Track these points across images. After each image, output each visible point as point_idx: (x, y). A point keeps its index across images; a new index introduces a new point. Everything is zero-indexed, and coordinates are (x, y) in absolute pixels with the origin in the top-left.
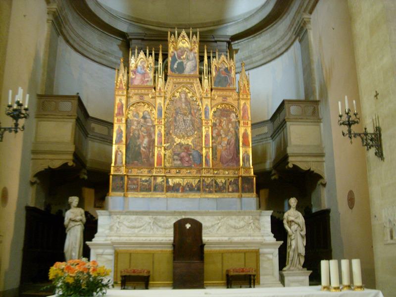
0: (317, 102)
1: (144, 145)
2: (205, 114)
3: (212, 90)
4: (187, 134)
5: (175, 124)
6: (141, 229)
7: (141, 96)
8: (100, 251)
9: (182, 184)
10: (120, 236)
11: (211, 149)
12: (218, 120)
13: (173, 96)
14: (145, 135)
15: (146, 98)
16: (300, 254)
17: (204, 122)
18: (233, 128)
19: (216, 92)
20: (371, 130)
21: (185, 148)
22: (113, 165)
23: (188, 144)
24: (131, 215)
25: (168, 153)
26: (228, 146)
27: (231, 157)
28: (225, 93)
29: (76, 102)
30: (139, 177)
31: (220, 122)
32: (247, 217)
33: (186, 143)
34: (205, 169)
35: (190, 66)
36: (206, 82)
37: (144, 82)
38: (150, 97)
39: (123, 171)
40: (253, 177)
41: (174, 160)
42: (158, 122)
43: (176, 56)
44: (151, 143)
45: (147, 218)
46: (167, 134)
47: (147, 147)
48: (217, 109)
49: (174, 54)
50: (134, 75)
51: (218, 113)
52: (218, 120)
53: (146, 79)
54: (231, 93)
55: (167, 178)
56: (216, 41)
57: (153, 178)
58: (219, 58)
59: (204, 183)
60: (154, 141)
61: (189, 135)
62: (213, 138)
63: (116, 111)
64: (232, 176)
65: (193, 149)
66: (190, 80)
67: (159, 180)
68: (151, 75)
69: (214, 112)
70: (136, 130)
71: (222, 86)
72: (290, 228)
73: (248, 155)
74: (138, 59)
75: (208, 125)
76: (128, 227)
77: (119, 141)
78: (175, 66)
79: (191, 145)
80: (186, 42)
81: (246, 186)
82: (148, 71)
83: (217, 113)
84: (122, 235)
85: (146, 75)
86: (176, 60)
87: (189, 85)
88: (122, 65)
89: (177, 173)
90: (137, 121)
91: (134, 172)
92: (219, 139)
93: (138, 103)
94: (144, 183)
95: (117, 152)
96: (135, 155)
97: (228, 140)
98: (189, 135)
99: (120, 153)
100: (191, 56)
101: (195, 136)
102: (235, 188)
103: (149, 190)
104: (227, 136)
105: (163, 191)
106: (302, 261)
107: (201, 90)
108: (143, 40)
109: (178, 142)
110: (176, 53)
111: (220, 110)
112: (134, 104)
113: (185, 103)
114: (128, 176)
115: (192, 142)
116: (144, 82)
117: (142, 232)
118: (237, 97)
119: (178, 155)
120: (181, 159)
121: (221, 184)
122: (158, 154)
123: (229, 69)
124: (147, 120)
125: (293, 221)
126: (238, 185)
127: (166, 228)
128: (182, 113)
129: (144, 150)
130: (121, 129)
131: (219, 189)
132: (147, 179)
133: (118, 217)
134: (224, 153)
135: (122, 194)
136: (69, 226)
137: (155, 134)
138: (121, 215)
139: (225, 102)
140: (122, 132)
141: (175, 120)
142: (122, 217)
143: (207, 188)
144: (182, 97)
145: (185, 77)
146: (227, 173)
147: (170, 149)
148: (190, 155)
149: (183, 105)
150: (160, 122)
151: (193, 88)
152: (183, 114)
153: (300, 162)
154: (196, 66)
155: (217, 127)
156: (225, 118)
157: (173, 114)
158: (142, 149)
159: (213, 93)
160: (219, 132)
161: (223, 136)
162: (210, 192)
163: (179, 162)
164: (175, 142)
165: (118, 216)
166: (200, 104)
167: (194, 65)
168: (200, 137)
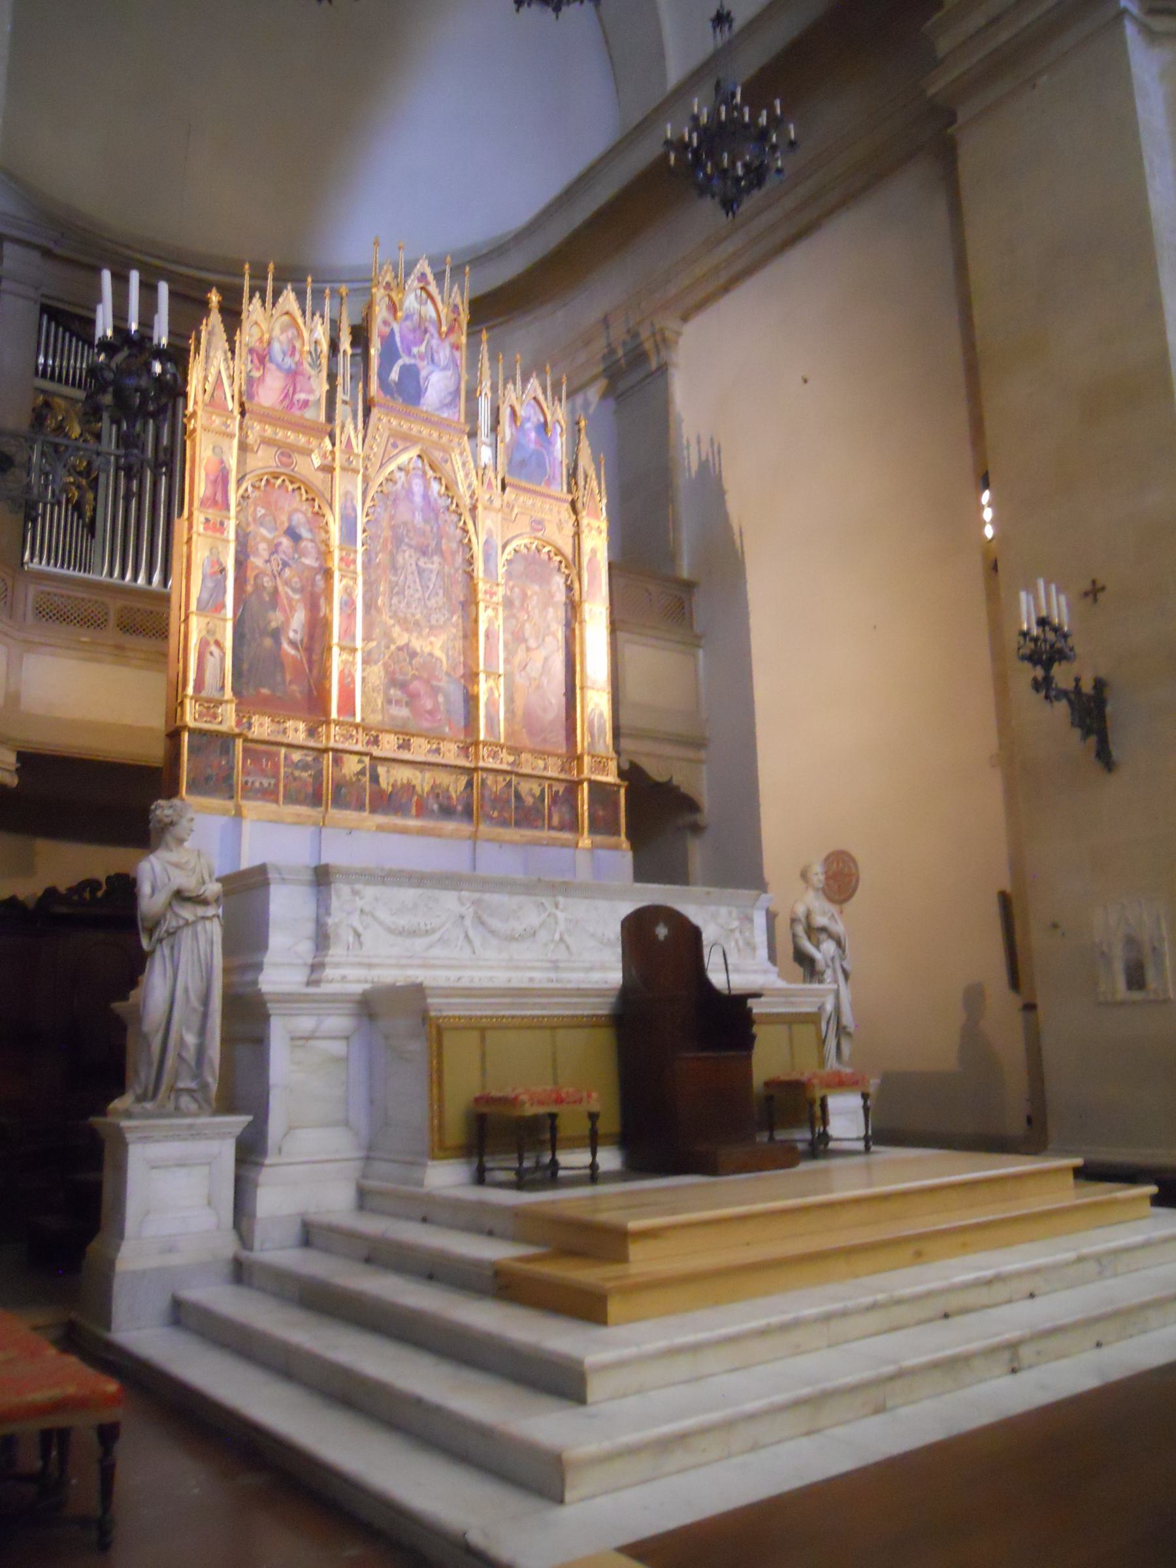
0: (689, 586)
1: (291, 635)
2: (487, 561)
4: (428, 618)
5: (394, 579)
6: (436, 936)
7: (286, 452)
8: (305, 1024)
9: (418, 788)
10: (370, 966)
11: (502, 679)
12: (517, 590)
14: (297, 597)
16: (845, 1028)
20: (1087, 687)
22: (190, 690)
23: (431, 655)
24: (400, 885)
30: (283, 750)
31: (524, 597)
32: (723, 910)
33: (427, 650)
34: (485, 744)
39: (228, 719)
40: (619, 786)
41: (389, 702)
42: (342, 559)
43: (398, 339)
44: (318, 628)
45: (449, 900)
47: (302, 641)
49: (392, 332)
50: (258, 369)
51: (519, 567)
52: (517, 590)
53: (302, 396)
59: (487, 793)
61: (433, 622)
64: (555, 774)
67: (352, 765)
68: (322, 387)
71: (529, 478)
75: (495, 599)
76: (390, 931)
78: (394, 375)
79: (438, 659)
80: (429, 302)
81: (601, 813)
82: (306, 366)
84: (375, 961)
85: (299, 378)
86: (398, 357)
89: (400, 747)
90: (269, 542)
92: (521, 655)
94: (297, 773)
95: (203, 645)
98: (433, 622)
99: (213, 648)
101: (454, 631)
102: (567, 817)
103: (316, 799)
105: (361, 807)
109: (401, 642)
110: (396, 327)
111: (525, 558)
113: (422, 511)
114: (246, 740)
115: (442, 648)
117: (437, 951)
119: (403, 686)
121: (529, 801)
122: (342, 673)
124: (303, 544)
125: (823, 929)
126: (574, 808)
127: (512, 938)
128: (413, 543)
129: (292, 652)
130: (221, 564)
132: (309, 759)
133: (355, 893)
135: (230, 804)
136: (171, 922)
138: (368, 883)
140: (223, 570)
141: (394, 567)
142: (370, 892)
143: (494, 809)
146: (541, 763)
147: (376, 663)
148: (435, 691)
149: (418, 517)
150: (347, 562)
152: (415, 549)
153: (648, 755)
154: (458, 390)
155: (515, 611)
156: (536, 588)
157: (385, 541)
158: (286, 646)
161: (532, 643)
162: (504, 823)
163: (403, 712)
165: (358, 887)
166: (470, 526)
167: (452, 388)
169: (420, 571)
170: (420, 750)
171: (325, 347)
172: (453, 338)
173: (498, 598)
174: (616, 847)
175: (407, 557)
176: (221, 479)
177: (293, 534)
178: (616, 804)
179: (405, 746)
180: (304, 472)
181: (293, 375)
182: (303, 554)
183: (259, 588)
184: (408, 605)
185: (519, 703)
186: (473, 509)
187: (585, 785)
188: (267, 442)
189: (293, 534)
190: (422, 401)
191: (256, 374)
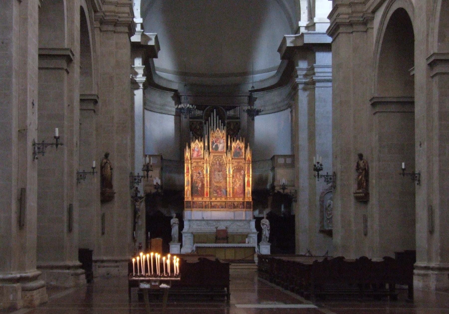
1: (199, 187)
3: (232, 159)
4: (220, 181)
7: (197, 163)
13: (213, 163)
15: (200, 164)
17: (228, 175)
18: (242, 177)
19: (234, 160)
21: (219, 188)
22: (185, 196)
23: (220, 186)
25: (212, 190)
26: (240, 187)
27: (241, 192)
28: (238, 160)
30: (198, 202)
31: (236, 175)
33: (219, 186)
35: (222, 146)
36: (229, 155)
37: (198, 156)
38: (202, 163)
39: (190, 199)
40: (251, 202)
43: (214, 141)
44: (203, 185)
46: (210, 181)
48: (235, 169)
49: (213, 141)
51: (235, 171)
53: (200, 154)
54: (241, 160)
55: (211, 202)
56: (240, 96)
57: (204, 202)
58: (236, 142)
59: (228, 205)
60: (204, 184)
62: (232, 183)
63: (185, 171)
65: (223, 188)
66: (221, 154)
68: (202, 152)
69: (233, 170)
70: (195, 179)
72: (263, 227)
73: (249, 191)
74: (195, 144)
77: (188, 185)
78: (214, 147)
82: (200, 150)
83: (234, 171)
86: (214, 144)
87: (221, 157)
88: (187, 147)
91: (195, 199)
92: (235, 184)
93: (196, 166)
95: (187, 190)
96: (194, 192)
97: (240, 184)
99: (188, 191)
100: (222, 141)
102: (242, 207)
103: (203, 208)
104: (239, 181)
105: (209, 208)
107: (226, 159)
109: (215, 185)
110: (214, 140)
112: (194, 167)
115: (222, 185)
116: (198, 156)
118: (244, 162)
120: (217, 193)
121: (236, 205)
122: (206, 191)
123: (241, 148)
124: (201, 174)
129: (200, 189)
134: (238, 190)
135: (190, 209)
137: (204, 181)
139: (238, 165)
144: (217, 163)
145: (219, 152)
146: (239, 199)
148: (221, 191)
151: (222, 158)
158: (199, 188)
159: (232, 161)
160: (235, 180)
161: (237, 182)
163: (216, 195)
164: (214, 185)
166: (226, 167)
168: (226, 182)
169: (218, 175)
170: (218, 199)
171: (203, 146)
172: (223, 138)
173: (231, 176)
174: (251, 211)
176: (188, 169)
177: (199, 173)
178: (251, 205)
179: (216, 199)
180: (200, 164)
181: (198, 152)
182: (201, 176)
183: (195, 181)
184: (217, 180)
185: (235, 191)
186: (227, 164)
187: (245, 202)
188: (195, 162)
189: (199, 173)
190: (219, 149)
191: (193, 153)
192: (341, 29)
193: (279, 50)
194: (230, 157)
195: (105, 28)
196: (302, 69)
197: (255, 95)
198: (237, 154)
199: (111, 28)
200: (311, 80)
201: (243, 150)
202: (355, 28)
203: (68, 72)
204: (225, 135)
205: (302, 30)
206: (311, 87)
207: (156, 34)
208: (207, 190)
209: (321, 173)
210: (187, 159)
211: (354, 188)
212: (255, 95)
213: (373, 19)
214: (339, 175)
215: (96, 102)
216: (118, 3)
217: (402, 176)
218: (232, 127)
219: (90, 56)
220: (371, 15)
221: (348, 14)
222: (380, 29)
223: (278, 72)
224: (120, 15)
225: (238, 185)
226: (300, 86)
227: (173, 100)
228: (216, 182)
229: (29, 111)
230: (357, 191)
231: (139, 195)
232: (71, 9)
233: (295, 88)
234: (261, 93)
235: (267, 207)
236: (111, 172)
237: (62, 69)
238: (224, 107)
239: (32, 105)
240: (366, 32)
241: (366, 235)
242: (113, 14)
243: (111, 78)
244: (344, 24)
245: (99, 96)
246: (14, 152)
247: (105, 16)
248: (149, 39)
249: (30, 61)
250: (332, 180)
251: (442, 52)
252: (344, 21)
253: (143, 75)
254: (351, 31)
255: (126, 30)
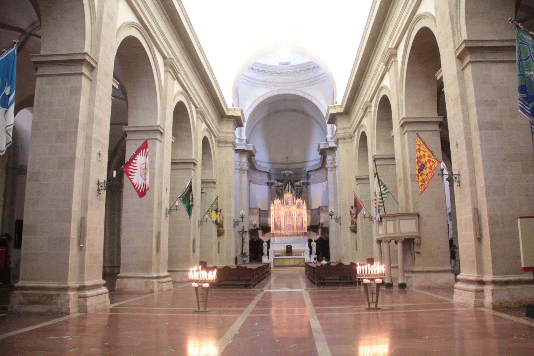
7: (278, 211)
8: (271, 252)
25: (285, 226)
29: (258, 210)
39: (274, 232)
44: (281, 224)
46: (285, 221)
68: (280, 206)
91: (277, 232)
96: (276, 227)
103: (281, 236)
106: (315, 253)
108: (276, 175)
120: (289, 228)
131: (298, 235)
145: (289, 206)
163: (288, 229)
168: (293, 222)
169: (289, 218)
170: (289, 231)
171: (280, 203)
175: (288, 217)
177: (279, 217)
181: (278, 206)
189: (279, 217)
192: (340, 141)
193: (318, 150)
194: (295, 207)
195: (220, 145)
196: (329, 160)
197: (310, 173)
198: (299, 206)
199: (224, 145)
200: (334, 166)
201: (302, 203)
202: (346, 140)
203: (194, 170)
204: (292, 196)
205: (329, 140)
206: (334, 169)
207: (253, 144)
208: (283, 226)
209: (333, 216)
210: (272, 210)
211: (349, 224)
212: (310, 173)
213: (354, 136)
214: (342, 218)
215: (215, 183)
216: (227, 132)
217: (364, 218)
218: (298, 191)
219: (212, 160)
220: (354, 134)
221: (343, 133)
222: (357, 141)
223: (320, 161)
224: (228, 138)
225: (299, 223)
226: (329, 169)
227: (267, 177)
228: (288, 222)
229: (164, 194)
230: (351, 226)
231: (245, 230)
232: (196, 140)
233: (326, 170)
234: (314, 172)
235: (318, 235)
236: (223, 220)
237: (191, 169)
238: (294, 180)
239: (166, 190)
240: (352, 142)
241: (357, 250)
242: (225, 138)
243: (223, 170)
244: (340, 139)
245: (217, 180)
246: (155, 214)
247: (220, 139)
248: (250, 147)
249: (165, 169)
250: (339, 220)
251: (378, 154)
252: (341, 137)
253: (247, 166)
254: (344, 142)
255: (231, 145)
